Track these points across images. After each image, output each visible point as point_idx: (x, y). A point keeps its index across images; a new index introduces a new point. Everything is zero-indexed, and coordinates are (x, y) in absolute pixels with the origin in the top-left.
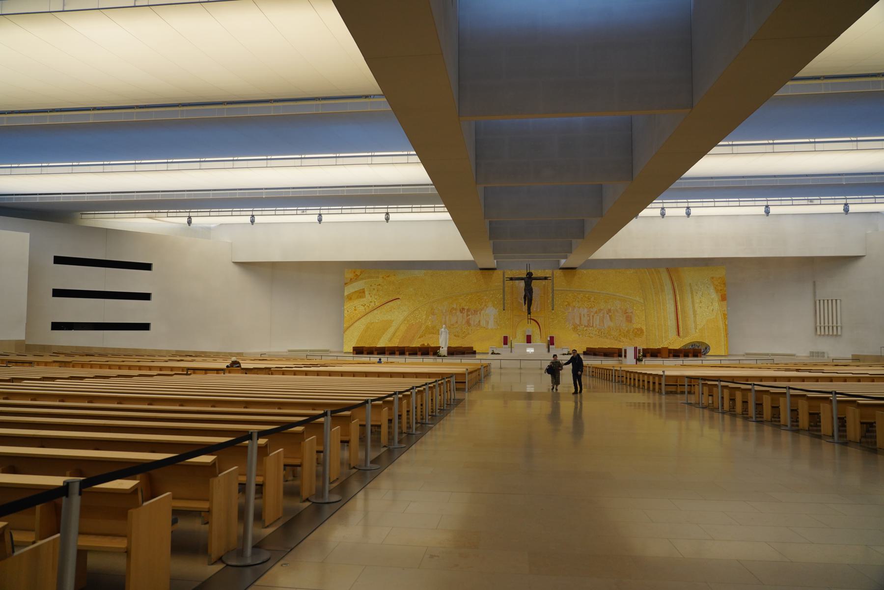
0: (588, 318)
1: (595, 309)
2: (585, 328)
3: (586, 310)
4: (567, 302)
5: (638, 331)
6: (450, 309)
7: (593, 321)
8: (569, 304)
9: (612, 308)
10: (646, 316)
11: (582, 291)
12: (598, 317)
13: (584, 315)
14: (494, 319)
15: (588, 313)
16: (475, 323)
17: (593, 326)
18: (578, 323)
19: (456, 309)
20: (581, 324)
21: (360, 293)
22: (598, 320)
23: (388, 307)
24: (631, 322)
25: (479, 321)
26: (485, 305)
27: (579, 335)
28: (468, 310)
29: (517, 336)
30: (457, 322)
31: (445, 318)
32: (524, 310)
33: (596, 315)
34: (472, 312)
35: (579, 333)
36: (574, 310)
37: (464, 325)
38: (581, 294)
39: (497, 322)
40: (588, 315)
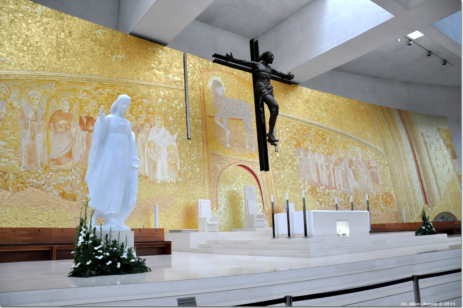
0: (328, 171)
1: (334, 158)
2: (327, 191)
4: (295, 139)
5: (387, 197)
6: (50, 113)
7: (334, 177)
9: (353, 159)
10: (391, 174)
11: (311, 124)
12: (340, 171)
14: (169, 157)
15: (327, 164)
17: (335, 188)
18: (317, 182)
19: (68, 117)
20: (320, 184)
22: (341, 179)
24: (378, 183)
26: (147, 120)
29: (220, 203)
30: (70, 155)
31: (33, 138)
32: (228, 145)
33: (336, 167)
35: (321, 200)
38: (313, 130)
39: (175, 164)
40: (327, 166)
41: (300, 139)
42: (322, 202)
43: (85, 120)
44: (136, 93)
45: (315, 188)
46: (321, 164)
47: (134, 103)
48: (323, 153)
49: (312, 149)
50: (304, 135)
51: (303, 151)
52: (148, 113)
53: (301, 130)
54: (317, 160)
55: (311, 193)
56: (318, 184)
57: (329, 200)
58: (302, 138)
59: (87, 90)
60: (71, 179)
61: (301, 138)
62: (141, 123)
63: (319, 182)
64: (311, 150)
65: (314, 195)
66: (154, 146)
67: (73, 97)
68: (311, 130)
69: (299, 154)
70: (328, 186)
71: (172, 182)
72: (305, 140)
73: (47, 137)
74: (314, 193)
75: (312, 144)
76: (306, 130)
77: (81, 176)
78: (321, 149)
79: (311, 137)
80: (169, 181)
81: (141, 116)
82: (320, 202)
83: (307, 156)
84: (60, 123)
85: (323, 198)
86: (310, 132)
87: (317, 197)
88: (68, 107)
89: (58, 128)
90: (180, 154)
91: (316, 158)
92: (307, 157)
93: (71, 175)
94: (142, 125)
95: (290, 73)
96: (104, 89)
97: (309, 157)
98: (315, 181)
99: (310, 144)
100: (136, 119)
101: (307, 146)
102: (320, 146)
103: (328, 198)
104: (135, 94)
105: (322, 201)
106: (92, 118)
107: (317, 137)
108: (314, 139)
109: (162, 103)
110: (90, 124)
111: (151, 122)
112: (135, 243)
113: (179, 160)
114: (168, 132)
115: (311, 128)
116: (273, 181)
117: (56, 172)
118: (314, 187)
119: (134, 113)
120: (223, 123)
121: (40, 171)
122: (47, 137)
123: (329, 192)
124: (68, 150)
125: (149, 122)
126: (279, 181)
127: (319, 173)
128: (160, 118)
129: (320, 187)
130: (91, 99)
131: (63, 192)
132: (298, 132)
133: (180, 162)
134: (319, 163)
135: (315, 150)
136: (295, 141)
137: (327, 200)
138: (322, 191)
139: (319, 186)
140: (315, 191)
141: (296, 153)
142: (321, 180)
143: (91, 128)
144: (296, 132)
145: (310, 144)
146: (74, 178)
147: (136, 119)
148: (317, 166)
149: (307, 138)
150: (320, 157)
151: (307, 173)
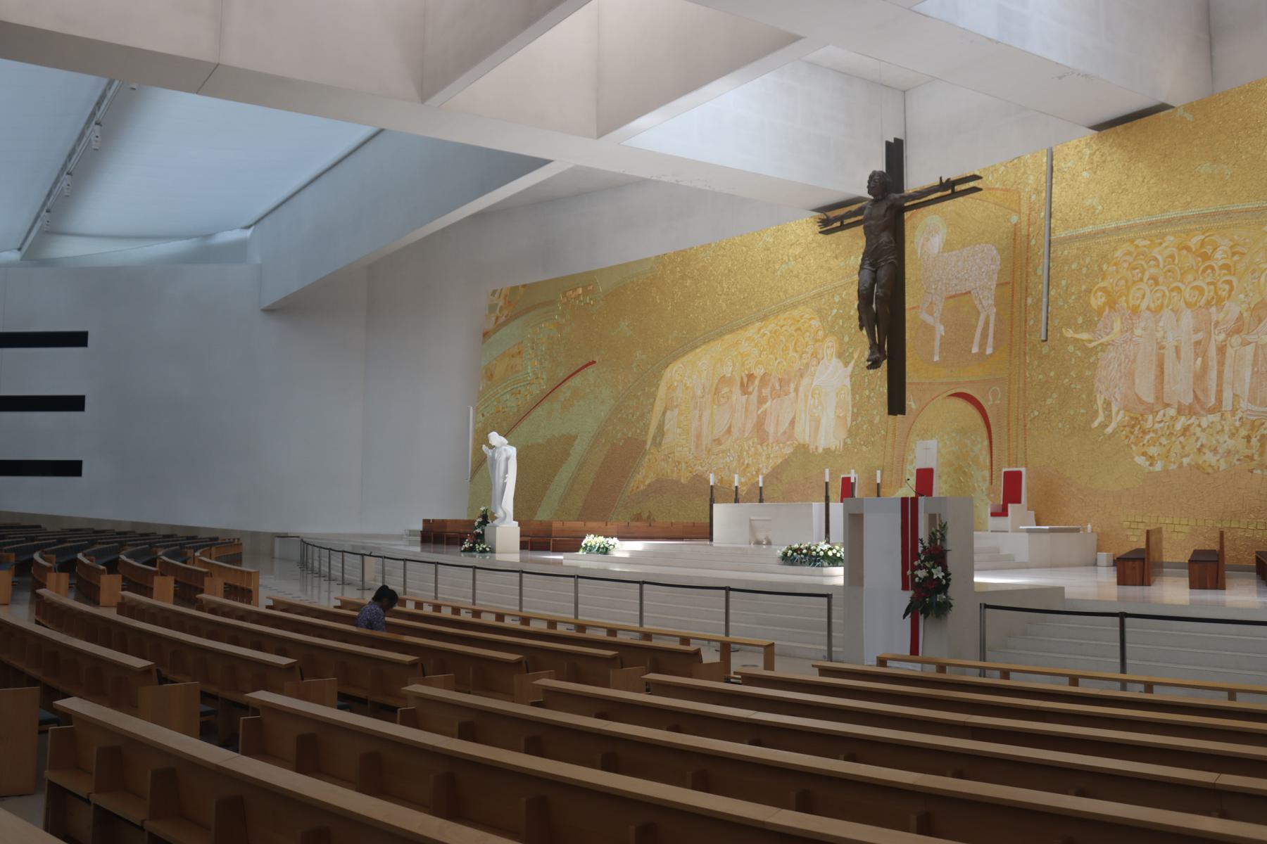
2: (1182, 422)
3: (1188, 319)
4: (1104, 289)
8: (1112, 304)
13: (1177, 349)
14: (836, 407)
16: (781, 430)
18: (1149, 398)
21: (513, 356)
23: (568, 394)
25: (792, 422)
27: (1152, 459)
28: (764, 380)
30: (729, 431)
32: (936, 358)
34: (773, 388)
35: (1153, 451)
36: (1131, 329)
37: (748, 439)
39: (845, 417)
41: (1117, 285)
42: (1156, 459)
43: (745, 380)
44: (803, 315)
45: (1140, 419)
46: (1176, 344)
47: (799, 332)
48: (1188, 305)
49: (1152, 306)
50: (1134, 269)
51: (1122, 319)
52: (817, 341)
53: (1127, 258)
54: (1165, 332)
55: (1124, 433)
56: (1153, 404)
57: (1183, 447)
58: (1127, 281)
59: (750, 337)
60: (729, 461)
61: (1123, 282)
62: (805, 361)
63: (1157, 398)
64: (1148, 308)
65: (1132, 437)
66: (819, 393)
67: (736, 353)
68: (1161, 244)
69: (1108, 331)
70: (1190, 407)
71: (838, 447)
72: (1134, 282)
73: (712, 413)
74: (1136, 432)
75: (1157, 288)
76: (1146, 249)
77: (738, 456)
78: (1188, 289)
79: (1158, 266)
80: (834, 447)
81: (807, 350)
82: (1151, 457)
83: (1132, 328)
84: (723, 392)
85: (1164, 446)
86: (1155, 253)
87: (1141, 444)
88: (731, 369)
89: (722, 399)
90: (853, 399)
91: (1160, 329)
92: (1132, 332)
93: (729, 456)
94: (807, 364)
95: (941, 178)
96: (766, 327)
97: (1138, 332)
98: (1145, 398)
99: (1148, 292)
100: (801, 357)
101: (1137, 299)
102: (1182, 287)
103: (1180, 442)
104: (802, 317)
105: (1159, 455)
106: (753, 374)
107: (1179, 261)
108: (1165, 270)
109: (836, 317)
110: (750, 384)
111: (818, 356)
112: (521, 536)
113: (851, 409)
114: (841, 364)
115: (1162, 239)
116: (1022, 416)
117: (717, 455)
118: (1138, 416)
119: (798, 349)
120: (931, 314)
121: (704, 456)
122: (712, 413)
123: (1189, 425)
124: (729, 423)
125: (816, 357)
126: (1036, 413)
127: (1162, 373)
128: (830, 344)
129: (1157, 412)
130: (753, 348)
131: (722, 478)
132: (1115, 268)
133: (853, 412)
134: (1170, 343)
135: (1162, 304)
136: (1101, 298)
137: (1177, 448)
138: (1162, 425)
139: (1157, 409)
140: (1140, 428)
141: (1100, 330)
142: (1166, 387)
143: (751, 389)
144: (1110, 268)
145: (1148, 292)
146: (732, 459)
147: (801, 357)
148: (1162, 351)
149: (1143, 274)
150: (1177, 321)
151: (1123, 380)
